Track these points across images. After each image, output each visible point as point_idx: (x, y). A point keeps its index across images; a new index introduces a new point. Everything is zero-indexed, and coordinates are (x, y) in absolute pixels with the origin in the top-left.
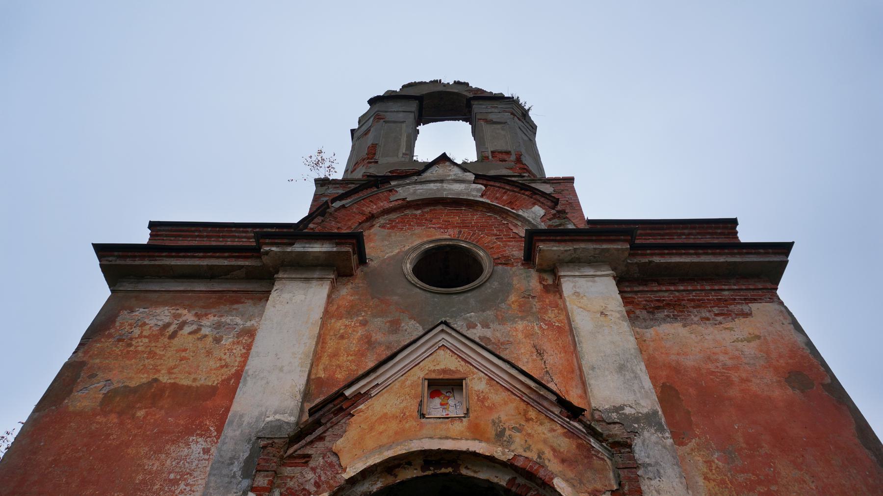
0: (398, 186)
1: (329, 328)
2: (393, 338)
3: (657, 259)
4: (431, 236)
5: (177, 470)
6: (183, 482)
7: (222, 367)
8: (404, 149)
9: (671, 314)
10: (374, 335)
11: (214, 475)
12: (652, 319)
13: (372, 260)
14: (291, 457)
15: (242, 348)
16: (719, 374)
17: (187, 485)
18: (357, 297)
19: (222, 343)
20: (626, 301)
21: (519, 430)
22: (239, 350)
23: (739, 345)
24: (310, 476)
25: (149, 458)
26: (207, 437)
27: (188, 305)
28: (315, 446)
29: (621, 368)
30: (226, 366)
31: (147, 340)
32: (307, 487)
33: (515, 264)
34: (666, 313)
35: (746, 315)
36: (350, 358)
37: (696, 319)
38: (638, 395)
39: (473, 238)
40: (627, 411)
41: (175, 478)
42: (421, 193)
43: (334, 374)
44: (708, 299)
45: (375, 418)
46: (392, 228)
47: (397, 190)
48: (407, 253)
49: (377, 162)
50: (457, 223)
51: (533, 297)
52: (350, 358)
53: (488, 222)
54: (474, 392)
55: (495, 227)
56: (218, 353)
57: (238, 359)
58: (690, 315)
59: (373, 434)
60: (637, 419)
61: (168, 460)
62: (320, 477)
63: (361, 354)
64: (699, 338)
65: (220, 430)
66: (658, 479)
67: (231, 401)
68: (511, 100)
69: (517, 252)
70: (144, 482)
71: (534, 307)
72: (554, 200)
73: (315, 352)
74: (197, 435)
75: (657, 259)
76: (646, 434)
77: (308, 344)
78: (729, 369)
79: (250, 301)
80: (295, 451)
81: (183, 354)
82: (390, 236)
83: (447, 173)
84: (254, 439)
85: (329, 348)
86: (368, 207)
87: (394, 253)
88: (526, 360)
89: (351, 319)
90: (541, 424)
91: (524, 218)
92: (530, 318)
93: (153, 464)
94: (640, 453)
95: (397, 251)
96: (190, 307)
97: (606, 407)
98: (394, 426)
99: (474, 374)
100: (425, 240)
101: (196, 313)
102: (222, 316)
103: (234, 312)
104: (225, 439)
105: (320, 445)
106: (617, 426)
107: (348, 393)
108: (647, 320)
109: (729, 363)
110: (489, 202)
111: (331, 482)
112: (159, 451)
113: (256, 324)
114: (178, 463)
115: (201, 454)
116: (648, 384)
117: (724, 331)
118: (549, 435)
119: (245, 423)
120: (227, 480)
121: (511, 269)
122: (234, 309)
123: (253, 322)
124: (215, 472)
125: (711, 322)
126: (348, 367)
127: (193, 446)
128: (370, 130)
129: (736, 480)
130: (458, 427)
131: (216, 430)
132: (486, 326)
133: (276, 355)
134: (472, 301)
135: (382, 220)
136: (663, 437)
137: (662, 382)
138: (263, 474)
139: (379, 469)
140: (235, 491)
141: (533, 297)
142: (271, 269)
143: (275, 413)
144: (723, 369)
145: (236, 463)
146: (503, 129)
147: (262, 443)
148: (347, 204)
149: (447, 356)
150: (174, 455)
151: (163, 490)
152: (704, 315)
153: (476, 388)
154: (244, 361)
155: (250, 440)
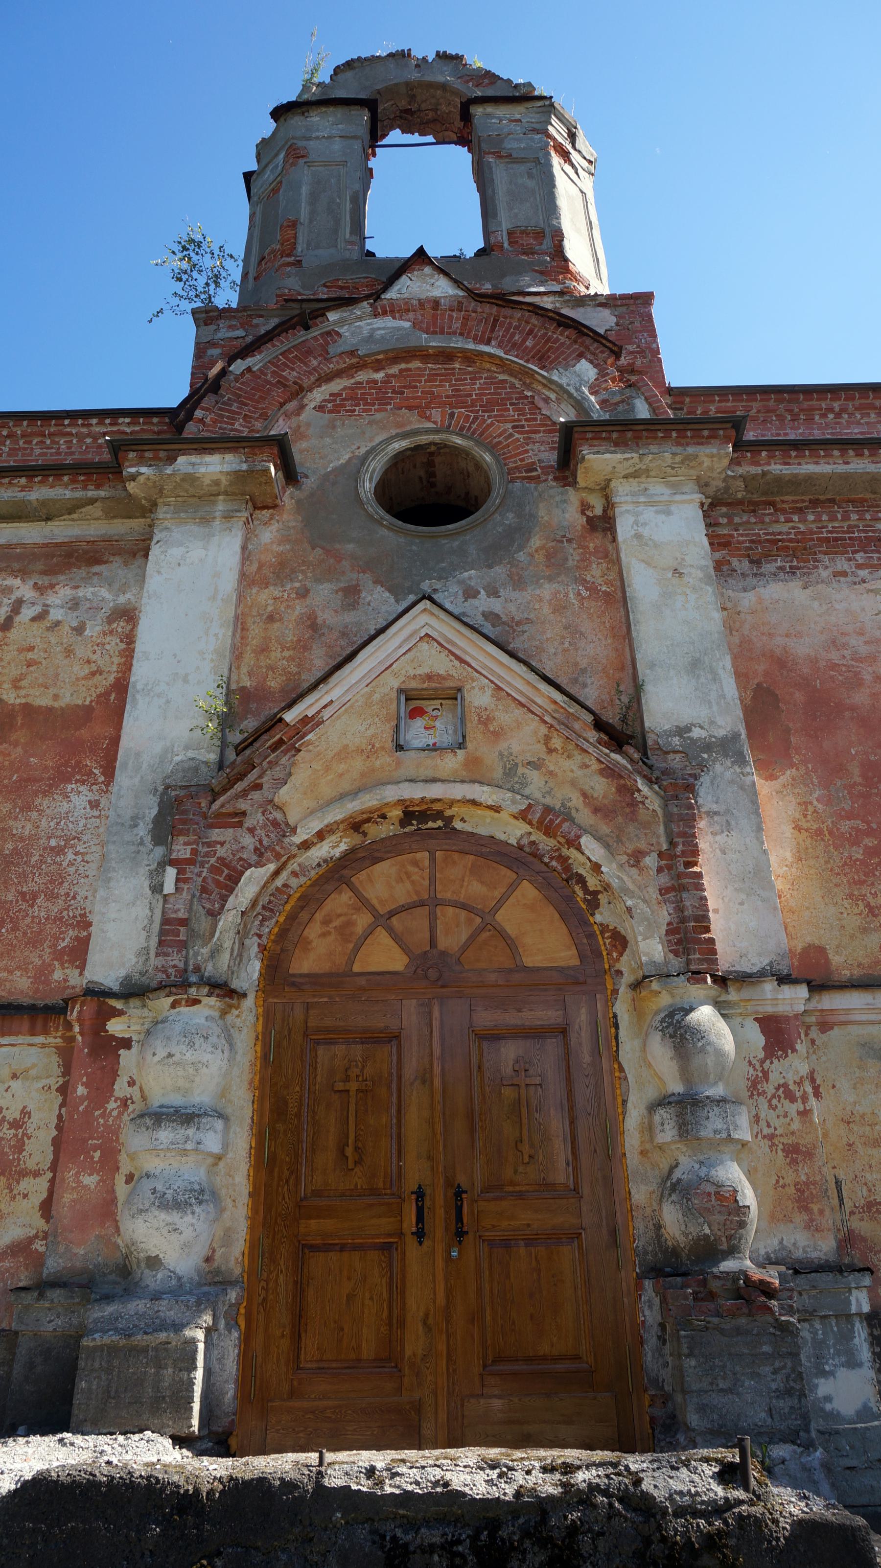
0: (341, 322)
1: (249, 603)
2: (349, 618)
3: (776, 468)
4: (403, 425)
5: (59, 833)
6: (71, 850)
7: (93, 674)
8: (348, 230)
9: (788, 565)
10: (319, 614)
11: (114, 842)
12: (755, 575)
13: (306, 476)
14: (218, 815)
15: (118, 641)
16: (844, 669)
17: (76, 854)
18: (288, 547)
19: (86, 633)
20: (717, 542)
21: (536, 765)
22: (114, 644)
24: (248, 841)
25: (16, 818)
26: (92, 784)
27: (19, 571)
28: (250, 797)
29: (695, 666)
30: (99, 672)
32: (245, 856)
33: (543, 477)
34: (779, 564)
36: (286, 654)
37: (824, 574)
38: (715, 708)
39: (474, 426)
40: (696, 733)
41: (59, 846)
42: (382, 337)
43: (265, 680)
44: (850, 538)
45: (331, 754)
46: (336, 410)
47: (341, 331)
48: (364, 459)
49: (299, 262)
50: (447, 397)
51: (569, 541)
52: (286, 654)
53: (500, 394)
54: (473, 710)
55: (511, 404)
56: (82, 652)
57: (117, 660)
58: (817, 567)
59: (329, 778)
60: (708, 747)
61: (44, 820)
62: (261, 841)
63: (302, 646)
64: (825, 607)
65: (109, 772)
66: (727, 833)
67: (118, 726)
68: (547, 103)
69: (547, 454)
70: (15, 852)
71: (570, 558)
72: (615, 349)
73: (234, 647)
74: (77, 781)
75: (776, 468)
76: (718, 768)
77: (220, 636)
78: (860, 660)
79: (117, 558)
80: (222, 806)
81: (30, 655)
82: (334, 427)
83: (428, 291)
84: (161, 788)
85: (253, 638)
86: (293, 369)
87: (342, 461)
88: (553, 651)
89: (283, 586)
90: (569, 757)
91: (560, 386)
92: (562, 577)
93: (23, 827)
95: (347, 457)
96: (23, 573)
97: (666, 727)
98: (358, 764)
99: (473, 680)
100: (394, 432)
101: (36, 584)
102: (77, 587)
103: (95, 580)
104: (119, 790)
105: (256, 795)
106: (678, 757)
107: (290, 717)
108: (748, 575)
109: (864, 650)
110: (502, 355)
111: (277, 848)
112: (27, 807)
113: (133, 600)
114: (58, 824)
115: (88, 810)
116: (730, 687)
117: (865, 595)
118: (579, 773)
119: (145, 766)
120: (133, 848)
121: (536, 488)
122: (96, 574)
123: (128, 596)
124: (115, 839)
125: (849, 579)
126: (284, 669)
127: (74, 797)
128: (281, 182)
129: (838, 829)
130: (451, 763)
131: (103, 774)
132: (493, 592)
133: (175, 655)
134: (472, 550)
135: (318, 395)
136: (742, 773)
137: (756, 682)
138: (182, 839)
139: (341, 827)
140: (146, 862)
141: (569, 541)
142: (143, 502)
143: (187, 748)
144: (852, 659)
145: (141, 824)
146: (530, 176)
147: (173, 793)
148: (254, 365)
149: (433, 652)
150: (48, 811)
151: (45, 862)
152: (839, 568)
153: (476, 704)
154: (125, 664)
155: (156, 790)
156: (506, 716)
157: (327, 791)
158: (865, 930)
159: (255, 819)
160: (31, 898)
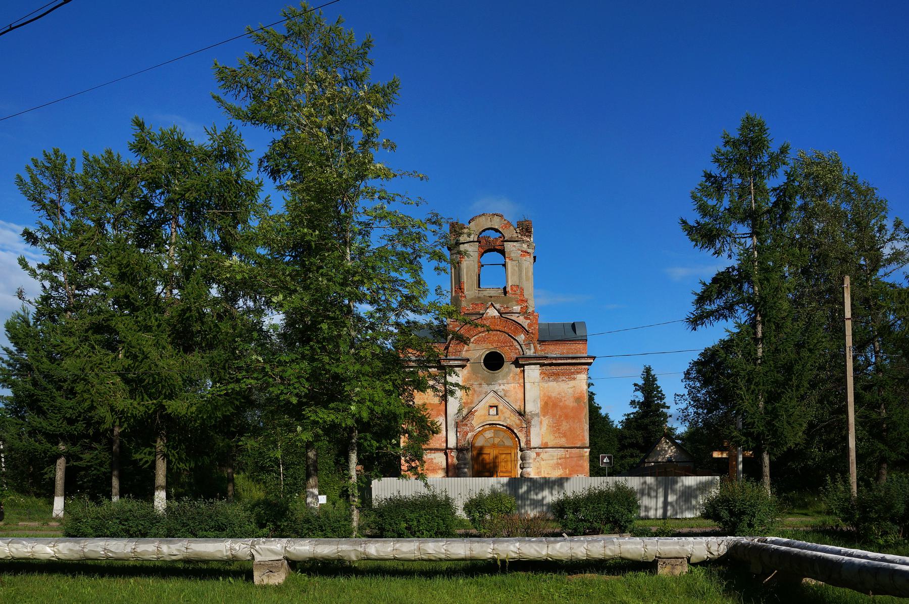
2: (480, 389)
24: (468, 428)
35: (574, 379)
60: (534, 414)
94: (533, 423)
98: (483, 417)
130: (497, 417)
156: (505, 410)
157: (479, 422)
159: (469, 425)
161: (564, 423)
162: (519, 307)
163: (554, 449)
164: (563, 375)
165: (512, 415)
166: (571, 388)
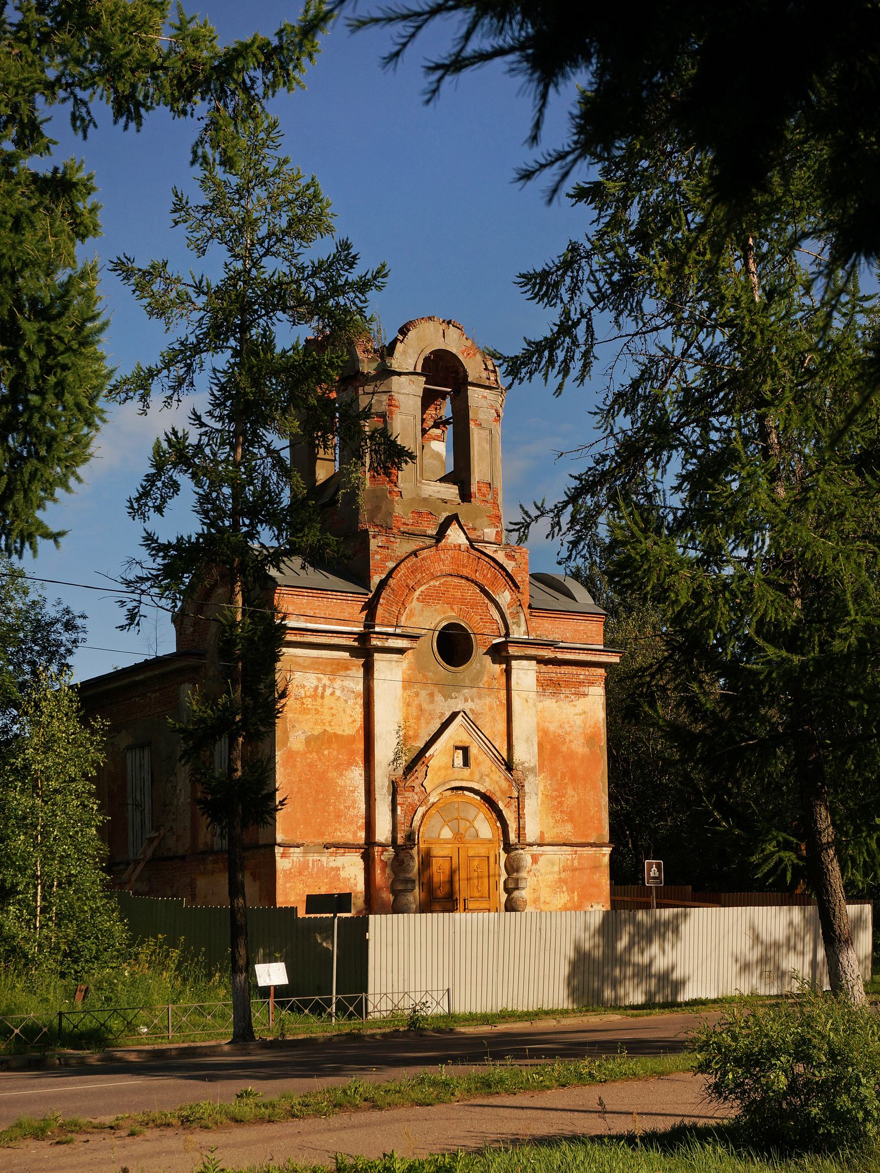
2: (431, 707)
4: (445, 613)
21: (488, 776)
23: (576, 717)
24: (416, 797)
30: (354, 721)
31: (310, 700)
35: (585, 695)
40: (526, 765)
56: (348, 711)
76: (530, 777)
98: (443, 773)
100: (443, 616)
109: (568, 730)
112: (341, 775)
130: (466, 772)
132: (473, 701)
135: (417, 593)
157: (437, 782)
158: (554, 827)
160: (348, 808)
161: (570, 791)
162: (494, 531)
163: (555, 848)
164: (567, 686)
165: (494, 768)
166: (580, 715)
